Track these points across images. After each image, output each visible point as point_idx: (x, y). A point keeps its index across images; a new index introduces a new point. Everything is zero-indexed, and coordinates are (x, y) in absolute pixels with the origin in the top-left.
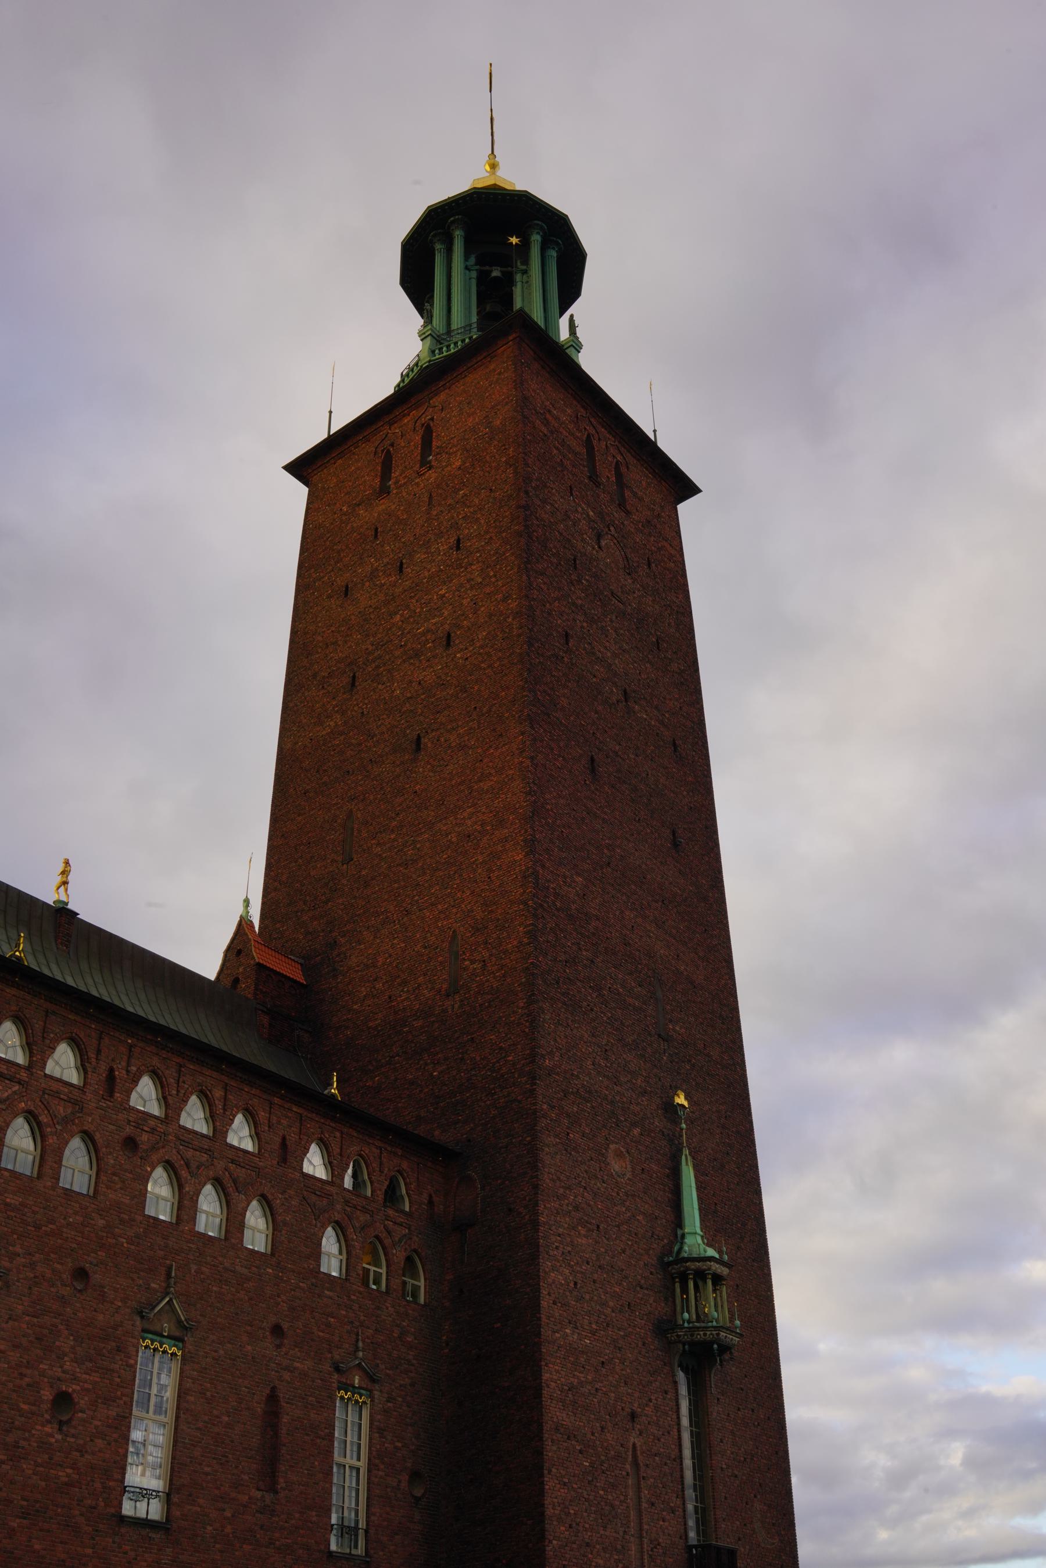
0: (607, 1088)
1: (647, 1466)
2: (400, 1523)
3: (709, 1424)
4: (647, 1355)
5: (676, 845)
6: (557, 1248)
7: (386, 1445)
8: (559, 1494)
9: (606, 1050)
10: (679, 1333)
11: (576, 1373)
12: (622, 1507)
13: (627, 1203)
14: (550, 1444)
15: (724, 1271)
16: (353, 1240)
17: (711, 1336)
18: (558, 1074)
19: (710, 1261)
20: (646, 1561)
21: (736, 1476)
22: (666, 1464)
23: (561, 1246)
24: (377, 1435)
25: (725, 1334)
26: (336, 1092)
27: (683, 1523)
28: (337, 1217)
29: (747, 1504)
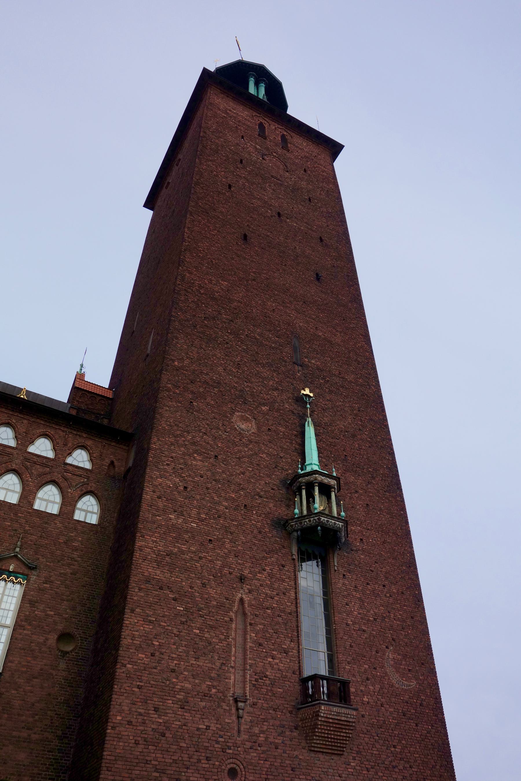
0: (236, 383)
1: (256, 615)
2: (41, 670)
3: (332, 591)
4: (262, 539)
5: (318, 278)
6: (168, 465)
7: (36, 612)
8: (142, 628)
9: (239, 364)
10: (292, 524)
11: (176, 544)
12: (220, 644)
13: (251, 446)
14: (136, 590)
15: (333, 482)
16: (27, 481)
17: (314, 521)
18: (186, 370)
19: (315, 474)
20: (248, 689)
21: (364, 631)
22: (279, 616)
23: (173, 464)
24: (28, 605)
25: (326, 519)
26: (25, 397)
27: (297, 662)
28: (14, 466)
29: (377, 652)
